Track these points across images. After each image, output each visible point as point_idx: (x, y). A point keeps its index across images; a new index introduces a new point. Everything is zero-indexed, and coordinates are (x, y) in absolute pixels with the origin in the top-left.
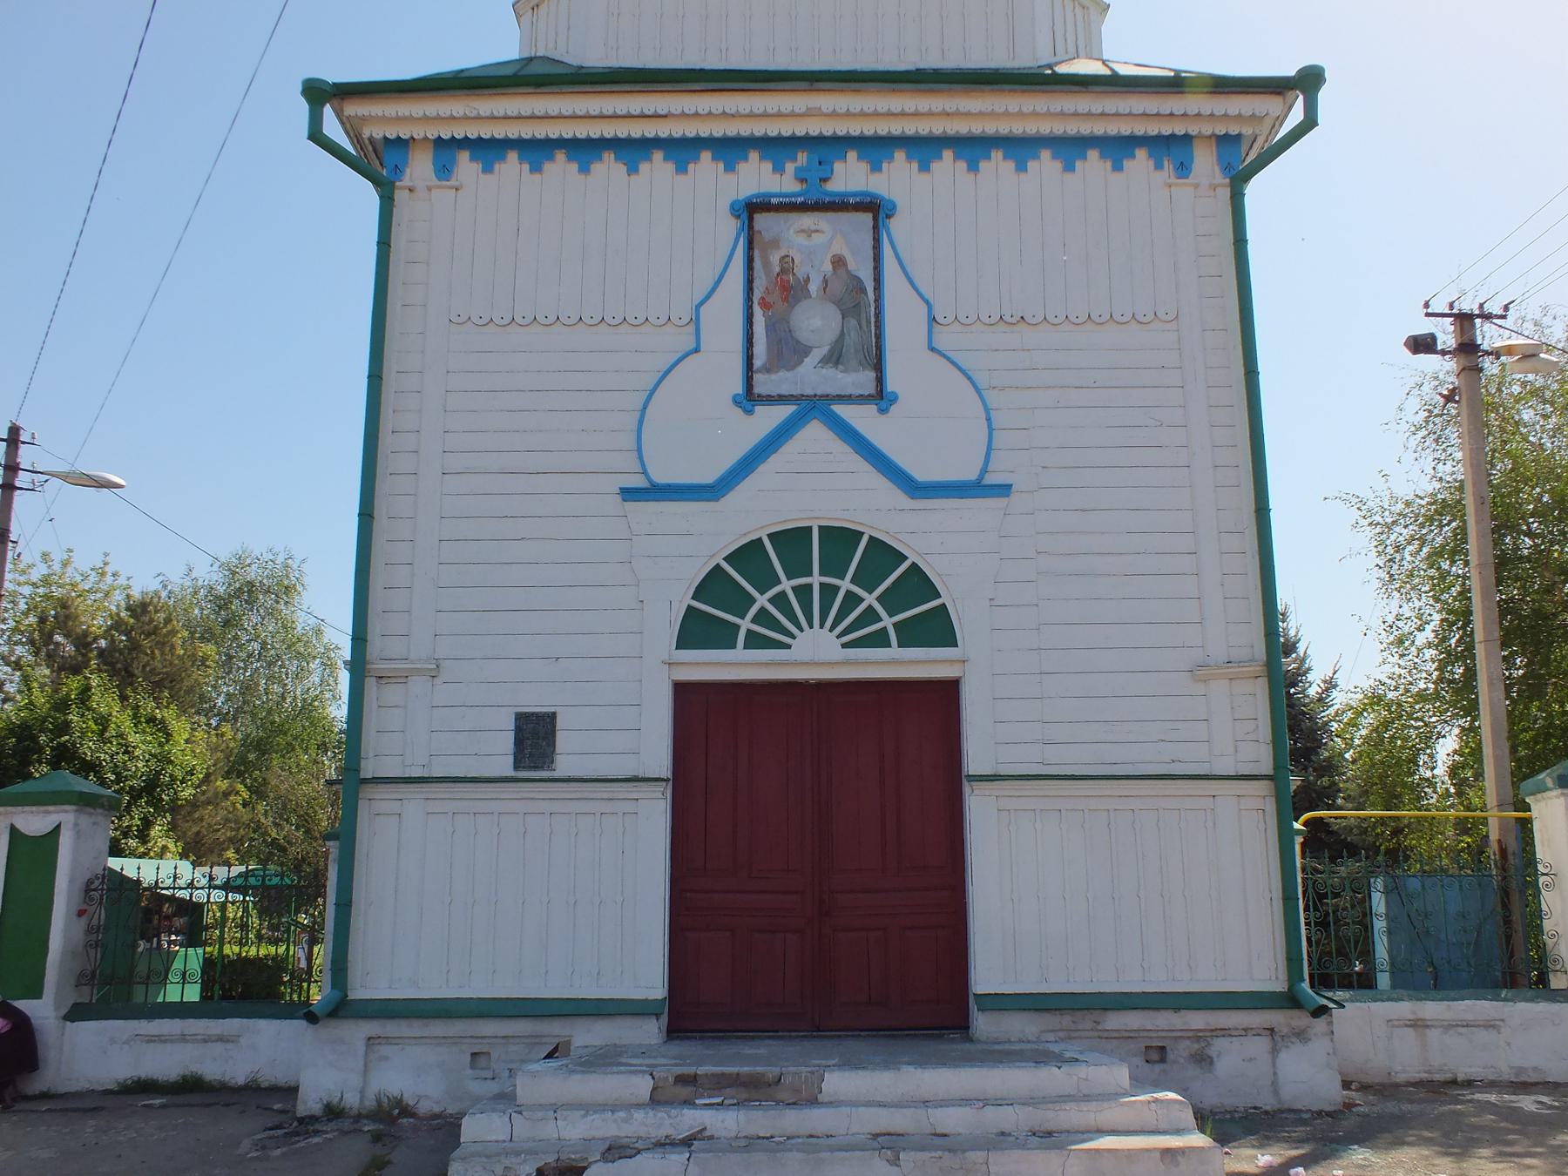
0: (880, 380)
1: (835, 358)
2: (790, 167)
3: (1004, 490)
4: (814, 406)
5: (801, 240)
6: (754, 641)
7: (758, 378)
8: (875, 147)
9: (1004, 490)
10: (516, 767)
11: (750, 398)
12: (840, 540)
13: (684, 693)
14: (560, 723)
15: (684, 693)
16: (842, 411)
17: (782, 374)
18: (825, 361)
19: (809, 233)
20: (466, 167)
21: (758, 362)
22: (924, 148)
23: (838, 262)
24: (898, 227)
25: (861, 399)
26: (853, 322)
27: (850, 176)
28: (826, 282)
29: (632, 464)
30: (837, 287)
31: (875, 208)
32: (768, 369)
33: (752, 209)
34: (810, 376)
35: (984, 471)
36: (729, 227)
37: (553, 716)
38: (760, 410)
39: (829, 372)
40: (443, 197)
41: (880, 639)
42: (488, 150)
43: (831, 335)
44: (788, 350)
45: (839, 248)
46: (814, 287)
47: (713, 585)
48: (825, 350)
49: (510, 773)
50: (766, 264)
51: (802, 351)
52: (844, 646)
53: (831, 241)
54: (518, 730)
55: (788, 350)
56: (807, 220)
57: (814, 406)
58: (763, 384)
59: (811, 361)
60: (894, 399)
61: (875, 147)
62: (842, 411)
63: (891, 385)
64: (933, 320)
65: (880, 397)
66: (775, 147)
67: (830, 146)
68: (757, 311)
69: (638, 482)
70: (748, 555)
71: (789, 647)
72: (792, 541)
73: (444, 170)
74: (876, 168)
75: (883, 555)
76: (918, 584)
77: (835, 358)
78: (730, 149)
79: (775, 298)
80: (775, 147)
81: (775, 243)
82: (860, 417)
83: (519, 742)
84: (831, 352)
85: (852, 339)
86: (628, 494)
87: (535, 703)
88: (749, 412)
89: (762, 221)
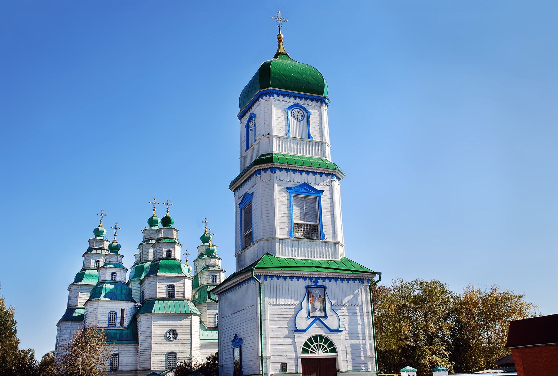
2: (313, 281)
4: (317, 319)
5: (315, 292)
6: (311, 352)
8: (324, 279)
9: (341, 331)
11: (309, 317)
12: (321, 337)
16: (322, 319)
18: (319, 311)
19: (316, 291)
20: (269, 279)
21: (310, 311)
22: (330, 279)
27: (320, 283)
29: (293, 326)
33: (308, 287)
34: (318, 314)
36: (305, 290)
40: (266, 283)
41: (327, 352)
42: (272, 277)
45: (320, 294)
47: (306, 344)
48: (319, 309)
51: (316, 309)
55: (314, 310)
56: (315, 289)
58: (311, 314)
59: (317, 311)
61: (324, 279)
65: (326, 317)
66: (311, 278)
67: (317, 279)
69: (295, 329)
70: (310, 340)
71: (316, 353)
72: (315, 337)
73: (266, 280)
74: (324, 281)
75: (327, 340)
76: (331, 344)
77: (320, 311)
78: (305, 278)
80: (311, 278)
81: (311, 293)
86: (295, 331)
87: (284, 362)
89: (310, 289)
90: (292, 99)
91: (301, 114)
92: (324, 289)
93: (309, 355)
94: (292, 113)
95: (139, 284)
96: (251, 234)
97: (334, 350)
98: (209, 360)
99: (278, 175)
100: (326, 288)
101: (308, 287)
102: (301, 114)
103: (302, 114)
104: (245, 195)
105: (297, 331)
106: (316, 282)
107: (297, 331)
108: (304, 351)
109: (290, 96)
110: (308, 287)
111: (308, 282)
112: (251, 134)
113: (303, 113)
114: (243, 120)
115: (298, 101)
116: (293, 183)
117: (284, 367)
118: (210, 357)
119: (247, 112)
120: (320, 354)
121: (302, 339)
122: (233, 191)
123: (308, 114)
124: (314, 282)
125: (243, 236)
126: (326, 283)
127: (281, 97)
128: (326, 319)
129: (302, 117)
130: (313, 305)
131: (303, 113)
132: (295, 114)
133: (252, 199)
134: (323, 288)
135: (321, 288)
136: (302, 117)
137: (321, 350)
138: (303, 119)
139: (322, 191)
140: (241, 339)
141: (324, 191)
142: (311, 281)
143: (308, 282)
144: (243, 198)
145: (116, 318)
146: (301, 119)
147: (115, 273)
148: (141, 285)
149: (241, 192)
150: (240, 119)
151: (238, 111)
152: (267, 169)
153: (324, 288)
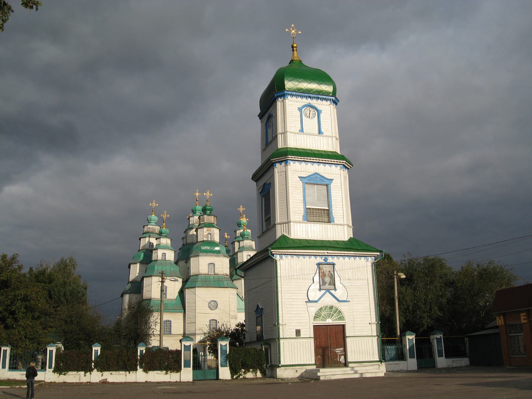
0: (335, 287)
1: (330, 284)
3: (349, 301)
5: (325, 268)
6: (322, 320)
7: (321, 287)
9: (349, 301)
10: (296, 336)
11: (320, 289)
13: (315, 326)
14: (301, 330)
15: (315, 326)
16: (330, 291)
17: (324, 286)
18: (329, 284)
19: (326, 267)
21: (321, 285)
23: (329, 271)
24: (335, 266)
25: (333, 290)
26: (331, 279)
27: (330, 260)
28: (328, 274)
30: (329, 275)
31: (333, 264)
32: (322, 286)
33: (319, 264)
35: (347, 299)
37: (300, 330)
38: (322, 291)
39: (329, 286)
43: (329, 281)
44: (324, 283)
45: (330, 270)
46: (327, 275)
49: (295, 337)
50: (321, 271)
51: (326, 283)
52: (332, 321)
53: (328, 269)
54: (296, 332)
56: (326, 266)
57: (328, 290)
60: (337, 290)
62: (330, 291)
63: (336, 288)
64: (340, 279)
65: (335, 289)
68: (320, 278)
73: (281, 258)
77: (330, 284)
79: (322, 276)
81: (322, 269)
82: (333, 292)
83: (296, 333)
84: (329, 283)
85: (331, 281)
87: (298, 328)
88: (320, 291)
90: (304, 99)
91: (313, 112)
92: (334, 266)
93: (319, 322)
94: (305, 112)
95: (185, 262)
96: (270, 218)
97: (342, 318)
98: (238, 327)
99: (292, 166)
100: (335, 264)
101: (319, 264)
102: (313, 112)
103: (314, 113)
104: (265, 184)
105: (309, 301)
106: (325, 260)
107: (309, 301)
108: (315, 318)
109: (302, 97)
110: (319, 264)
111: (320, 260)
112: (270, 131)
113: (314, 111)
114: (263, 120)
115: (309, 101)
116: (305, 173)
117: (298, 332)
118: (238, 325)
119: (266, 112)
120: (329, 321)
121: (313, 309)
122: (255, 181)
123: (319, 112)
124: (324, 260)
125: (264, 220)
126: (335, 260)
127: (294, 98)
128: (335, 291)
129: (314, 115)
130: (323, 280)
131: (314, 111)
132: (307, 112)
133: (270, 188)
134: (332, 264)
135: (330, 264)
136: (314, 115)
137: (331, 318)
138: (314, 117)
139: (332, 180)
140: (262, 309)
141: (333, 179)
142: (322, 259)
143: (320, 260)
144: (263, 187)
145: (167, 290)
146: (313, 117)
147: (165, 254)
148: (186, 263)
149: (262, 182)
150: (260, 119)
151: (259, 111)
152: (282, 161)
153: (333, 264)
